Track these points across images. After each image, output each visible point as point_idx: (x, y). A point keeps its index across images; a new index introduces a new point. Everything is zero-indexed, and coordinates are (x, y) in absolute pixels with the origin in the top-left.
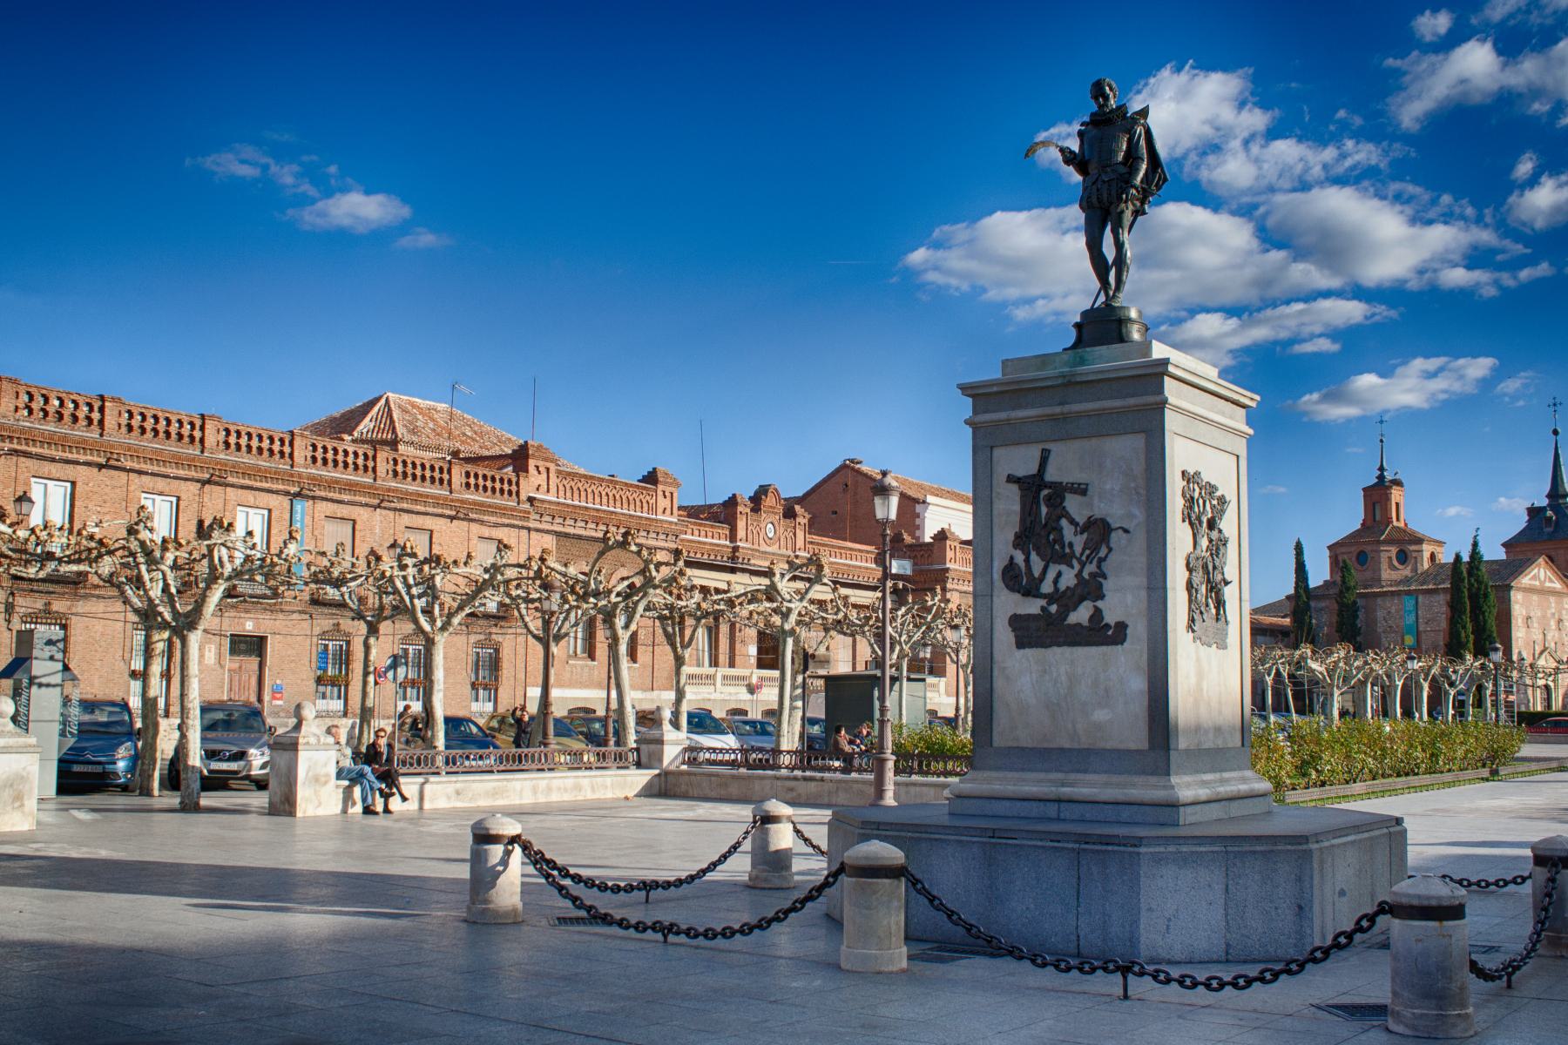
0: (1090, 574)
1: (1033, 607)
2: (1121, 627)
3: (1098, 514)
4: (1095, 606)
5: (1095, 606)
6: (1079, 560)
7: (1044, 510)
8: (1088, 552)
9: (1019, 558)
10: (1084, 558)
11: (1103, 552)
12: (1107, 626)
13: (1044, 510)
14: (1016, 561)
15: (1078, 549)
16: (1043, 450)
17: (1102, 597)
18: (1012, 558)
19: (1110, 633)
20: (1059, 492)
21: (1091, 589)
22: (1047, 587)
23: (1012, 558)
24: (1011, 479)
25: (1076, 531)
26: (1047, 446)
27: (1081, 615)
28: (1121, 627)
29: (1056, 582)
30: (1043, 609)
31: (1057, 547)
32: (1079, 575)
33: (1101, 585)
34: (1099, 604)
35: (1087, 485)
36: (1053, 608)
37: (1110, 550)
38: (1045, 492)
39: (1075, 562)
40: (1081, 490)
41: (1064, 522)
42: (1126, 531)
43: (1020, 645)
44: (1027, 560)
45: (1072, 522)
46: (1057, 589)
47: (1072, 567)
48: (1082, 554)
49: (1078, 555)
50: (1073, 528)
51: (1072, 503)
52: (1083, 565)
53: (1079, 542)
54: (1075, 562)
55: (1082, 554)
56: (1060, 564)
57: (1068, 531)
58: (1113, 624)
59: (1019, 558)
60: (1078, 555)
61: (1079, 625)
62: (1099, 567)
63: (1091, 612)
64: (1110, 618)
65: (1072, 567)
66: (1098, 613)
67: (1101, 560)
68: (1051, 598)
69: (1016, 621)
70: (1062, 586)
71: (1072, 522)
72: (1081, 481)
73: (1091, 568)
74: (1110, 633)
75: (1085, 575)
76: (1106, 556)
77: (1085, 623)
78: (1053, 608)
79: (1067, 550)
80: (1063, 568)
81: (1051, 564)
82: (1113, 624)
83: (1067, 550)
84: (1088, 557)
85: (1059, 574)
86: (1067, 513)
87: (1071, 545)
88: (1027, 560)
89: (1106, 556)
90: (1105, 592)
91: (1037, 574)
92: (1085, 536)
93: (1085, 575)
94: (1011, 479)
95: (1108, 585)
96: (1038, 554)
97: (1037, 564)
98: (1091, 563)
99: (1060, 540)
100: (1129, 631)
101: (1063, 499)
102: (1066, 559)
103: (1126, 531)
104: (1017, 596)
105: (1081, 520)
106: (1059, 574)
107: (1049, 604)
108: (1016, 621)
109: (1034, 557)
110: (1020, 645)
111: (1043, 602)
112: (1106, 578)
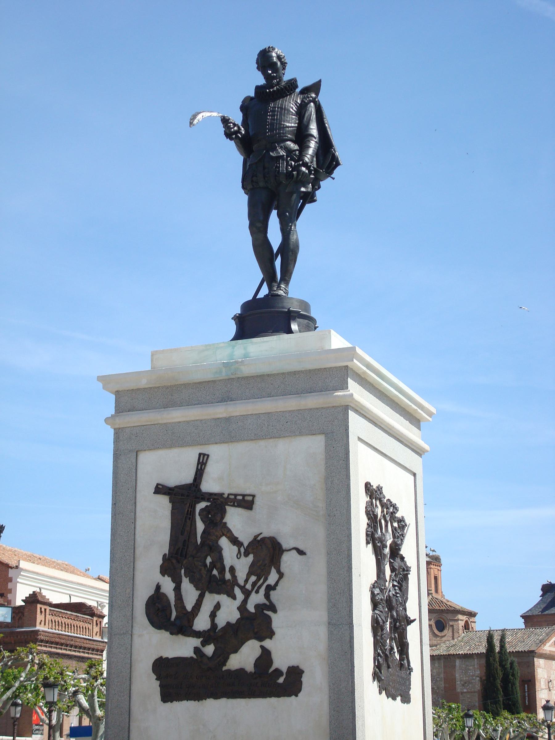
4: (262, 647)
5: (262, 647)
7: (200, 526)
8: (253, 578)
9: (168, 586)
10: (249, 586)
11: (273, 578)
13: (200, 526)
15: (241, 576)
18: (158, 587)
19: (281, 680)
23: (158, 587)
29: (213, 615)
32: (242, 608)
33: (269, 620)
34: (267, 643)
37: (281, 575)
38: (202, 505)
39: (237, 591)
42: (301, 552)
44: (178, 589)
45: (235, 541)
52: (247, 594)
54: (237, 591)
55: (246, 581)
56: (219, 593)
58: (284, 670)
59: (168, 586)
63: (258, 652)
67: (270, 588)
71: (235, 541)
73: (257, 598)
74: (281, 680)
75: (251, 608)
80: (223, 599)
81: (207, 594)
82: (284, 670)
85: (218, 607)
86: (229, 531)
87: (232, 569)
88: (178, 589)
91: (189, 607)
92: (251, 558)
93: (251, 608)
96: (191, 581)
98: (257, 592)
103: (301, 552)
106: (218, 607)
111: (196, 642)
112: (275, 611)
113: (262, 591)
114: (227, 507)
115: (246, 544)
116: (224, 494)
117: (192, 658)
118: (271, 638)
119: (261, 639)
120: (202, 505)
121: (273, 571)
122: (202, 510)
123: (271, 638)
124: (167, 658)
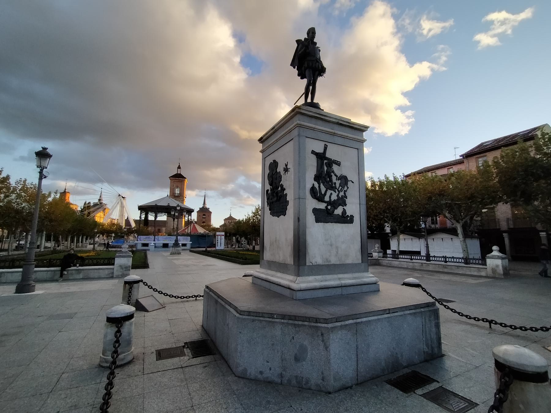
1: (322, 206)
2: (352, 217)
3: (344, 174)
4: (343, 208)
5: (343, 208)
6: (338, 191)
7: (325, 168)
8: (341, 187)
9: (316, 185)
10: (339, 189)
13: (325, 168)
15: (337, 185)
17: (346, 205)
18: (313, 185)
19: (348, 219)
20: (331, 163)
21: (342, 202)
22: (327, 198)
23: (313, 185)
24: (313, 152)
25: (337, 178)
26: (327, 144)
27: (339, 211)
28: (352, 217)
29: (330, 197)
30: (326, 207)
32: (338, 196)
34: (345, 207)
37: (348, 188)
38: (325, 161)
39: (336, 190)
40: (338, 164)
42: (353, 182)
43: (317, 221)
44: (319, 187)
45: (336, 175)
48: (339, 188)
49: (337, 188)
51: (335, 167)
53: (338, 183)
54: (336, 190)
55: (339, 188)
57: (334, 178)
59: (316, 185)
62: (345, 194)
64: (348, 213)
66: (344, 212)
67: (345, 191)
68: (329, 203)
69: (315, 211)
70: (332, 199)
73: (342, 194)
74: (348, 219)
75: (340, 196)
76: (347, 190)
77: (341, 214)
80: (332, 192)
83: (334, 185)
84: (341, 189)
85: (331, 194)
87: (335, 183)
88: (319, 187)
89: (347, 190)
93: (340, 196)
94: (313, 152)
95: (347, 201)
96: (323, 185)
97: (323, 189)
98: (342, 192)
99: (331, 180)
100: (354, 219)
102: (333, 188)
103: (353, 182)
106: (331, 194)
108: (315, 211)
109: (322, 185)
110: (317, 221)
111: (325, 205)
112: (347, 198)
113: (343, 191)
120: (325, 161)
121: (346, 187)
122: (326, 163)
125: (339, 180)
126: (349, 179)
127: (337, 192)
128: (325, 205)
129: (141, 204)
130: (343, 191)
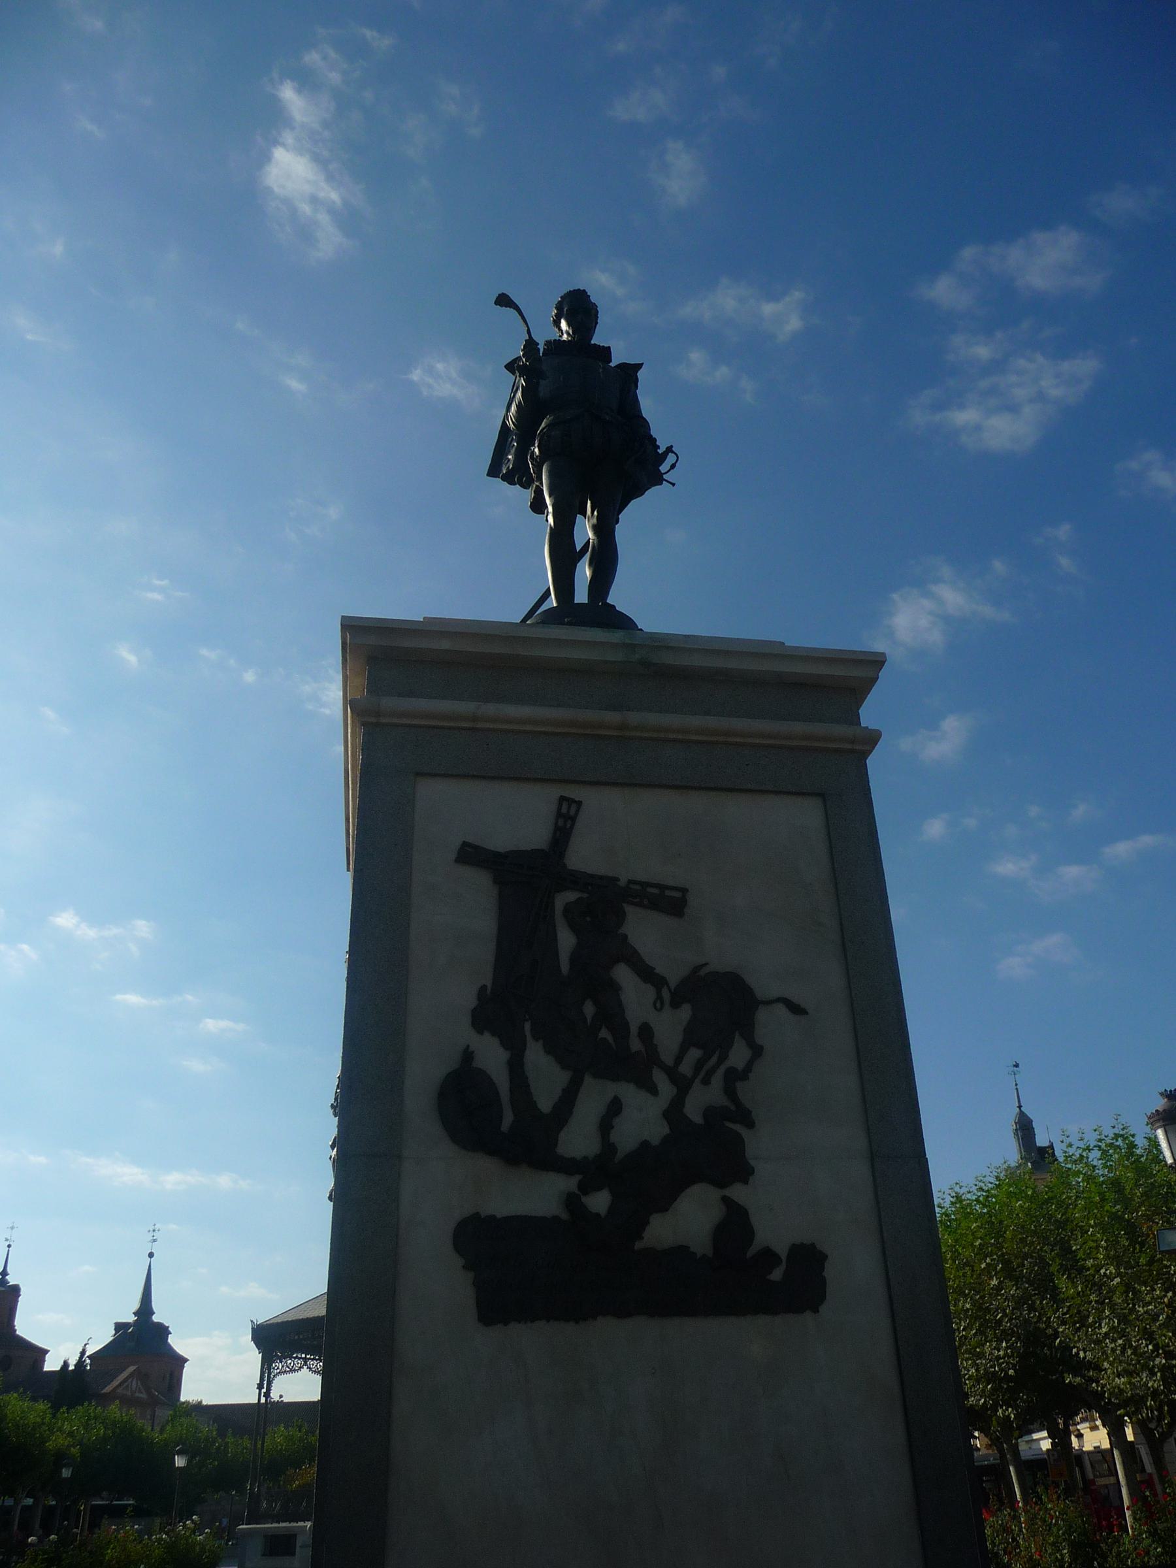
0: (709, 1113)
4: (726, 1200)
5: (726, 1200)
6: (672, 1074)
7: (566, 940)
8: (694, 1054)
10: (686, 1068)
11: (739, 1055)
12: (768, 1256)
13: (566, 940)
14: (479, 1063)
16: (562, 799)
17: (744, 1173)
18: (468, 1056)
19: (777, 1275)
23: (468, 1056)
24: (470, 855)
25: (659, 997)
29: (606, 1126)
30: (572, 1202)
31: (604, 1033)
32: (673, 1113)
34: (738, 1192)
35: (684, 891)
36: (599, 1202)
37: (757, 1051)
38: (571, 896)
41: (623, 974)
42: (796, 1009)
44: (516, 1066)
45: (647, 974)
46: (609, 1148)
47: (653, 1090)
48: (679, 1059)
49: (668, 1058)
50: (650, 992)
52: (683, 1086)
55: (679, 1059)
60: (668, 1058)
61: (681, 1252)
62: (730, 1091)
65: (653, 1090)
67: (734, 1078)
71: (647, 974)
72: (671, 882)
74: (777, 1275)
76: (748, 1068)
78: (599, 1202)
79: (636, 1045)
80: (629, 1093)
81: (588, 1080)
83: (636, 1045)
85: (615, 1107)
87: (646, 1031)
88: (516, 1066)
90: (752, 1163)
91: (545, 1103)
92: (685, 1013)
98: (706, 1082)
99: (612, 1015)
101: (621, 917)
103: (796, 1009)
104: (487, 1165)
105: (674, 975)
107: (585, 1188)
109: (536, 1056)
111: (566, 1183)
112: (750, 1125)
113: (717, 1080)
114: (625, 905)
115: (673, 981)
116: (617, 879)
117: (556, 1218)
118: (745, 1182)
119: (721, 1184)
120: (571, 896)
123: (745, 1182)
124: (493, 1217)
125: (675, 1004)
126: (764, 984)
127: (666, 1089)
128: (566, 1183)
129: (50, 1353)
130: (717, 1080)
